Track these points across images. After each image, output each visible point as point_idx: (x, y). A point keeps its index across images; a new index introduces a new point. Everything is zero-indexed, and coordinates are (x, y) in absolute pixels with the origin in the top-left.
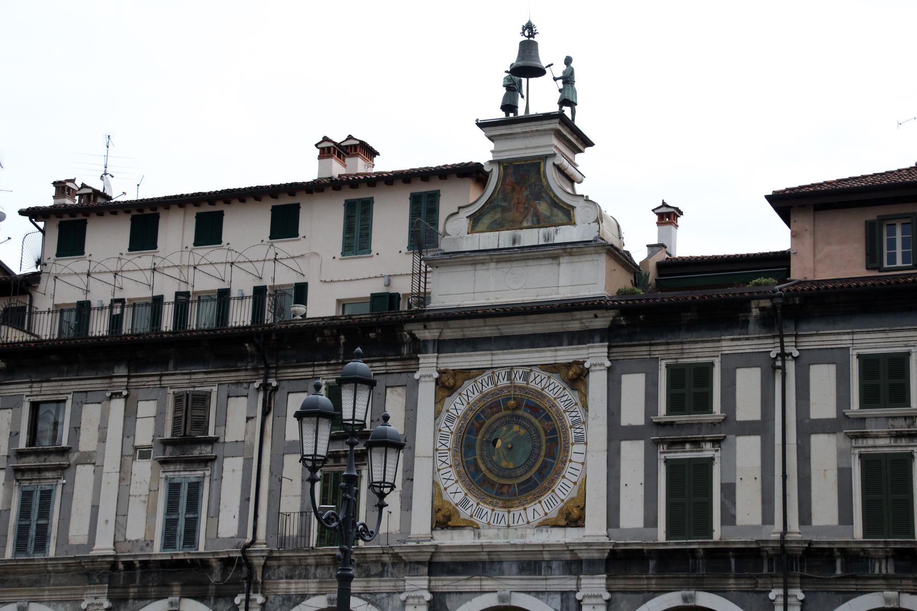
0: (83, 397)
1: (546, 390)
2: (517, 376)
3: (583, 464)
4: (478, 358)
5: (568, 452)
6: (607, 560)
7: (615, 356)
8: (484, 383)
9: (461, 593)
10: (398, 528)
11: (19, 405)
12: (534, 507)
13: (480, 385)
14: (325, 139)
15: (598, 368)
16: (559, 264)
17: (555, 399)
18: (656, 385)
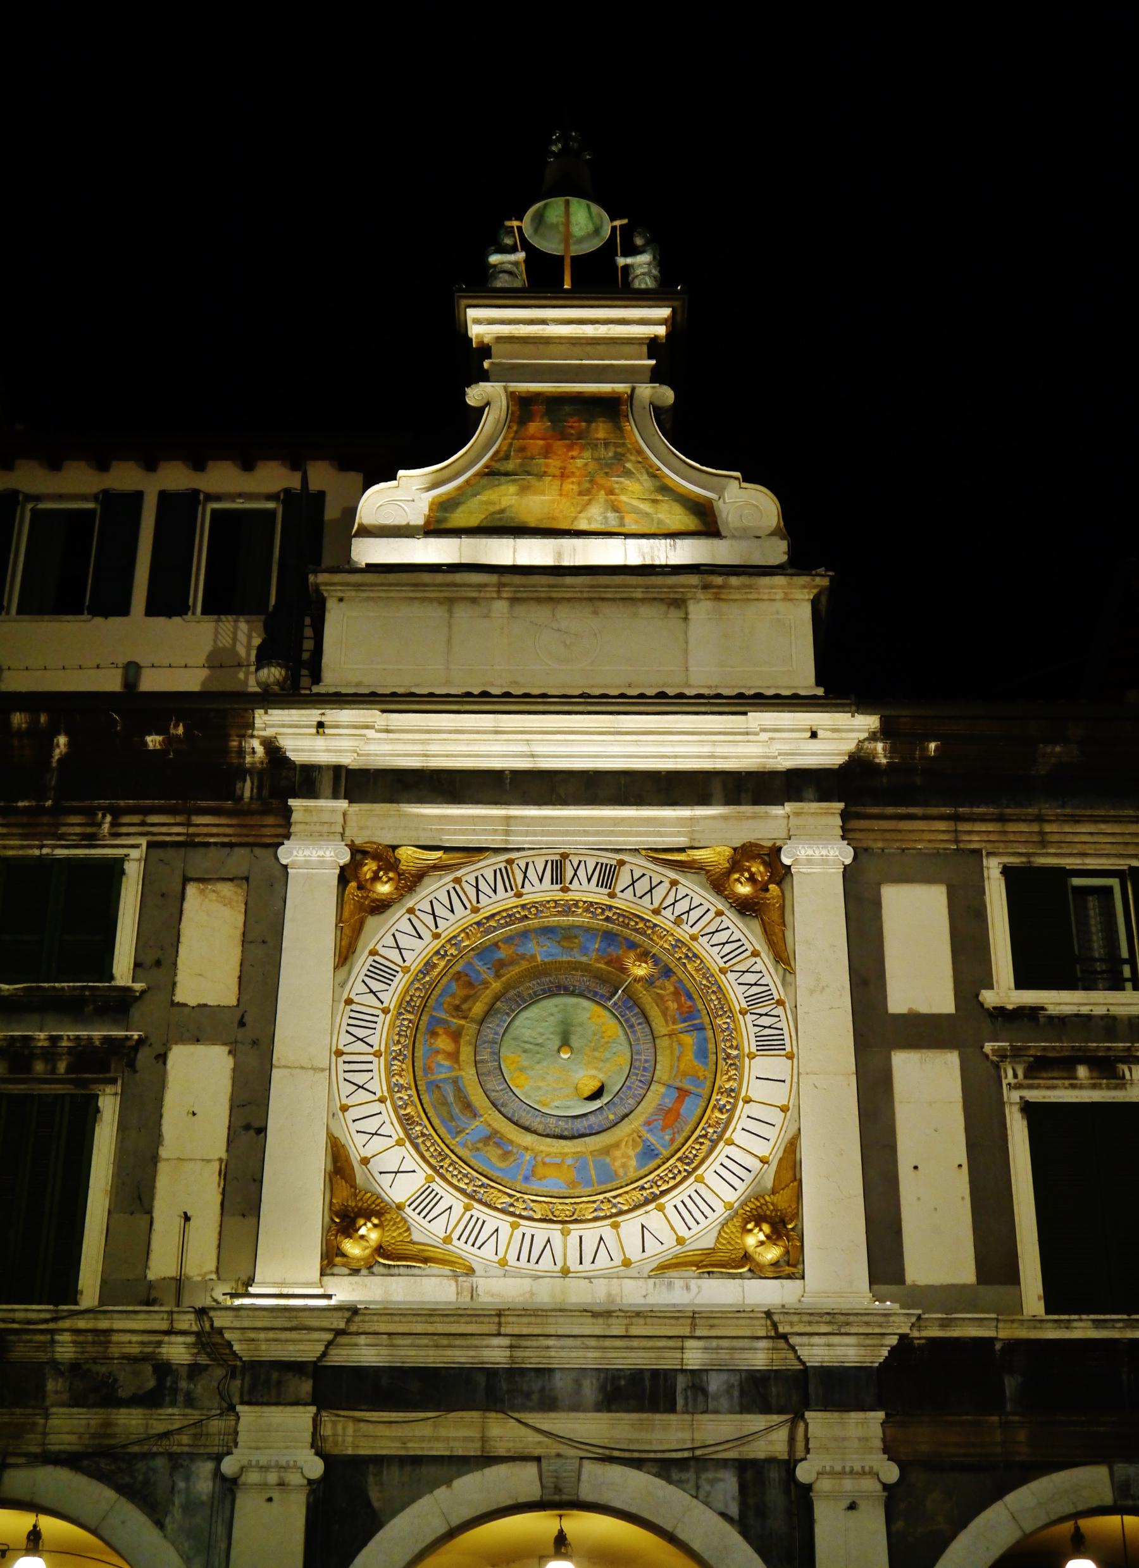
2: (581, 873)
3: (784, 1109)
8: (483, 885)
9: (416, 1461)
10: (212, 1266)
12: (643, 1220)
13: (472, 892)
16: (686, 619)
17: (694, 938)
18: (979, 914)
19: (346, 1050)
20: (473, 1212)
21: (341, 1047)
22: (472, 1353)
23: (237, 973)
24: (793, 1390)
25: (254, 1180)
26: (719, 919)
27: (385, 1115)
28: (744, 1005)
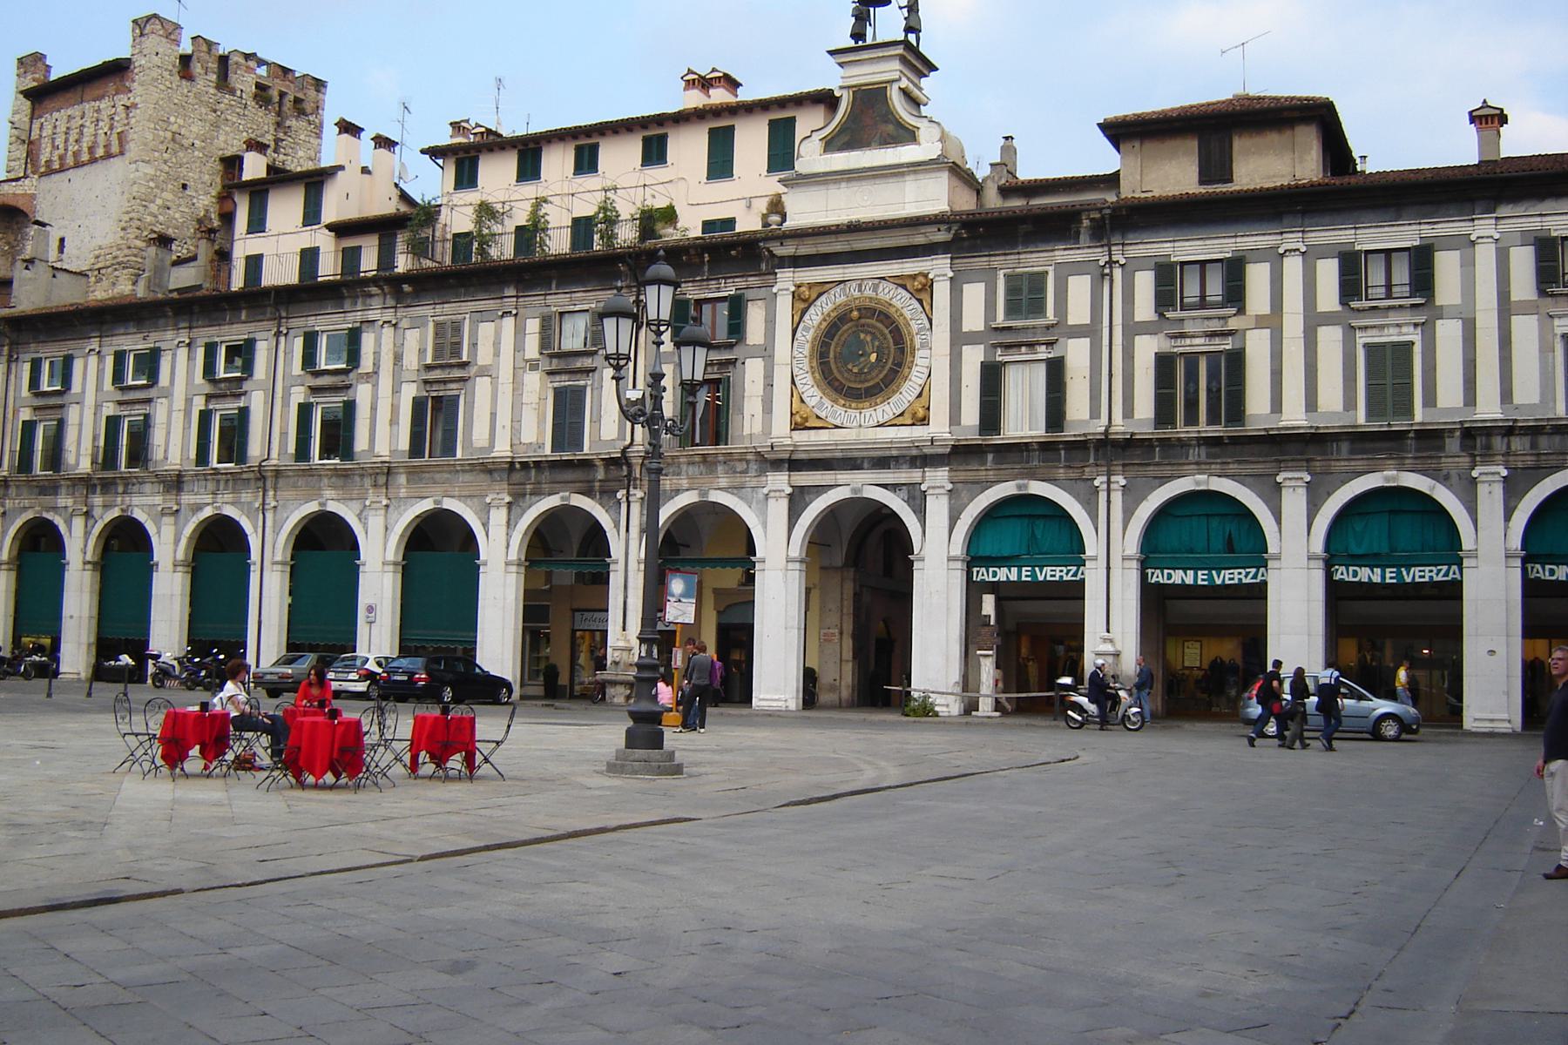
0: (481, 316)
11: (425, 325)
14: (690, 72)
24: (923, 460)
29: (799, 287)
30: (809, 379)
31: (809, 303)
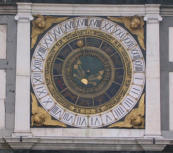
1: (114, 34)
2: (92, 23)
3: (142, 86)
4: (63, 8)
5: (130, 78)
6: (163, 151)
7: (166, 14)
8: (67, 26)
12: (107, 114)
13: (64, 28)
15: (153, 21)
17: (121, 40)
19: (34, 70)
20: (66, 112)
21: (33, 70)
22: (67, 147)
23: (6, 50)
25: (13, 104)
26: (127, 36)
27: (44, 88)
28: (133, 59)
29: (36, 17)
30: (45, 88)
31: (44, 31)
